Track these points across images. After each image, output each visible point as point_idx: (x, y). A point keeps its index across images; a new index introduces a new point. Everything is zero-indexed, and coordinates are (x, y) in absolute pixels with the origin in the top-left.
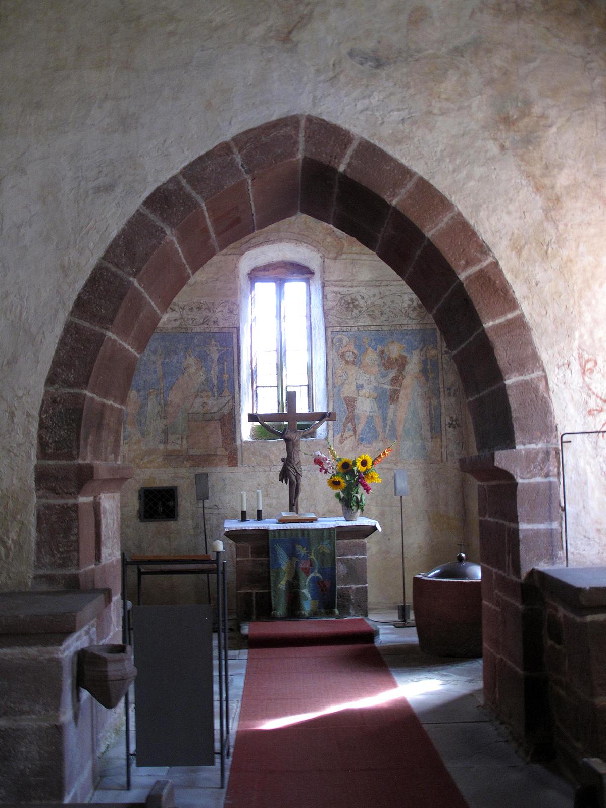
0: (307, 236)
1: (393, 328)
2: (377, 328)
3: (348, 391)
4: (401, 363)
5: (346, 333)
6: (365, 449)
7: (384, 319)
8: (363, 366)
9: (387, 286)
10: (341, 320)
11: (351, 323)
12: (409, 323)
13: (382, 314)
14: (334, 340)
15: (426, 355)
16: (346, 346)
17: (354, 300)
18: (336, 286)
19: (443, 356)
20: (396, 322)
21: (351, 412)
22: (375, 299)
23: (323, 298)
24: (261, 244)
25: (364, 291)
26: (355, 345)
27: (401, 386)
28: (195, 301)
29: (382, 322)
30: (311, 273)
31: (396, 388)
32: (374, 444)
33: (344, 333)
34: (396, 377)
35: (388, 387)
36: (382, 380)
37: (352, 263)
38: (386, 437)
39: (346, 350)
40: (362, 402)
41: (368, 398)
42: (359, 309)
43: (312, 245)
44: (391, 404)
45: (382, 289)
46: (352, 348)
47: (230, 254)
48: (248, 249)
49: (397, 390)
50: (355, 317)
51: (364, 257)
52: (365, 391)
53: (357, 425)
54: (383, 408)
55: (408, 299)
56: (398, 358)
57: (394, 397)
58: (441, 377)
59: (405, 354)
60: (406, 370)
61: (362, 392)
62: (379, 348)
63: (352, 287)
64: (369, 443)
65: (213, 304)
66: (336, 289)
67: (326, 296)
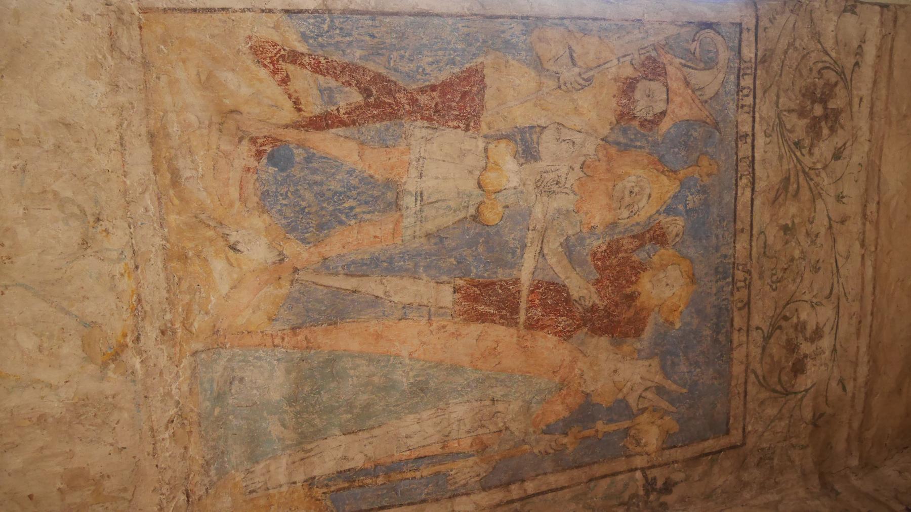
1: (740, 275)
2: (743, 214)
3: (512, 93)
4: (615, 321)
5: (732, 87)
6: (235, 175)
7: (771, 240)
8: (610, 159)
9: (863, 245)
10: (776, 65)
11: (765, 109)
12: (755, 334)
13: (785, 229)
14: (710, 33)
15: (643, 411)
16: (687, 84)
17: (832, 118)
18: (879, 49)
19: (638, 475)
20: (757, 284)
21: (413, 101)
22: (831, 201)
25: (856, 159)
26: (689, 123)
27: (533, 325)
29: (762, 232)
31: (523, 305)
32: (259, 221)
33: (732, 78)
34: (568, 300)
35: (526, 272)
36: (553, 244)
38: (301, 275)
39: (674, 85)
40: (463, 154)
41: (480, 186)
42: (807, 142)
44: (456, 290)
45: (854, 226)
46: (682, 110)
49: (515, 310)
50: (781, 124)
52: (510, 172)
53: (352, 131)
54: (433, 254)
55: (822, 320)
56: (638, 303)
57: (488, 300)
58: (560, 479)
59: (648, 333)
60: (594, 340)
61: (504, 154)
62: (676, 225)
63: (872, 114)
64: (265, 195)
66: (870, 52)
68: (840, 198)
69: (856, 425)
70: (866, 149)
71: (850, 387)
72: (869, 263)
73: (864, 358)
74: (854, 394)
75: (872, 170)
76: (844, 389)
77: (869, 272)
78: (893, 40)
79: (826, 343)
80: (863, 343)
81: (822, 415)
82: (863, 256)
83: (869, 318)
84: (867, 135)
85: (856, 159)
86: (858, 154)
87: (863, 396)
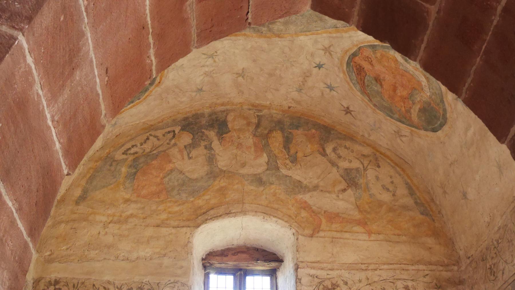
0: (277, 210)
9: (376, 270)
22: (361, 285)
23: (296, 283)
24: (220, 216)
25: (347, 275)
28: (135, 280)
30: (279, 260)
37: (332, 242)
43: (283, 220)
45: (370, 273)
47: (183, 227)
48: (205, 221)
51: (347, 235)
65: (158, 284)
66: (313, 272)
67: (300, 280)
68: (360, 281)
69: (441, 268)
70: (343, 271)
71: (427, 272)
72: (382, 267)
73: (416, 267)
74: (430, 270)
75: (351, 267)
76: (427, 275)
77: (386, 267)
78: (308, 262)
79: (410, 284)
80: (411, 267)
81: (436, 285)
82: (380, 270)
83: (402, 266)
84: (339, 271)
85: (347, 275)
86: (346, 274)
87: (430, 266)
